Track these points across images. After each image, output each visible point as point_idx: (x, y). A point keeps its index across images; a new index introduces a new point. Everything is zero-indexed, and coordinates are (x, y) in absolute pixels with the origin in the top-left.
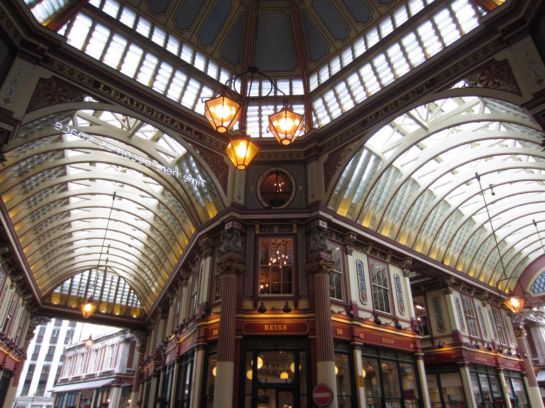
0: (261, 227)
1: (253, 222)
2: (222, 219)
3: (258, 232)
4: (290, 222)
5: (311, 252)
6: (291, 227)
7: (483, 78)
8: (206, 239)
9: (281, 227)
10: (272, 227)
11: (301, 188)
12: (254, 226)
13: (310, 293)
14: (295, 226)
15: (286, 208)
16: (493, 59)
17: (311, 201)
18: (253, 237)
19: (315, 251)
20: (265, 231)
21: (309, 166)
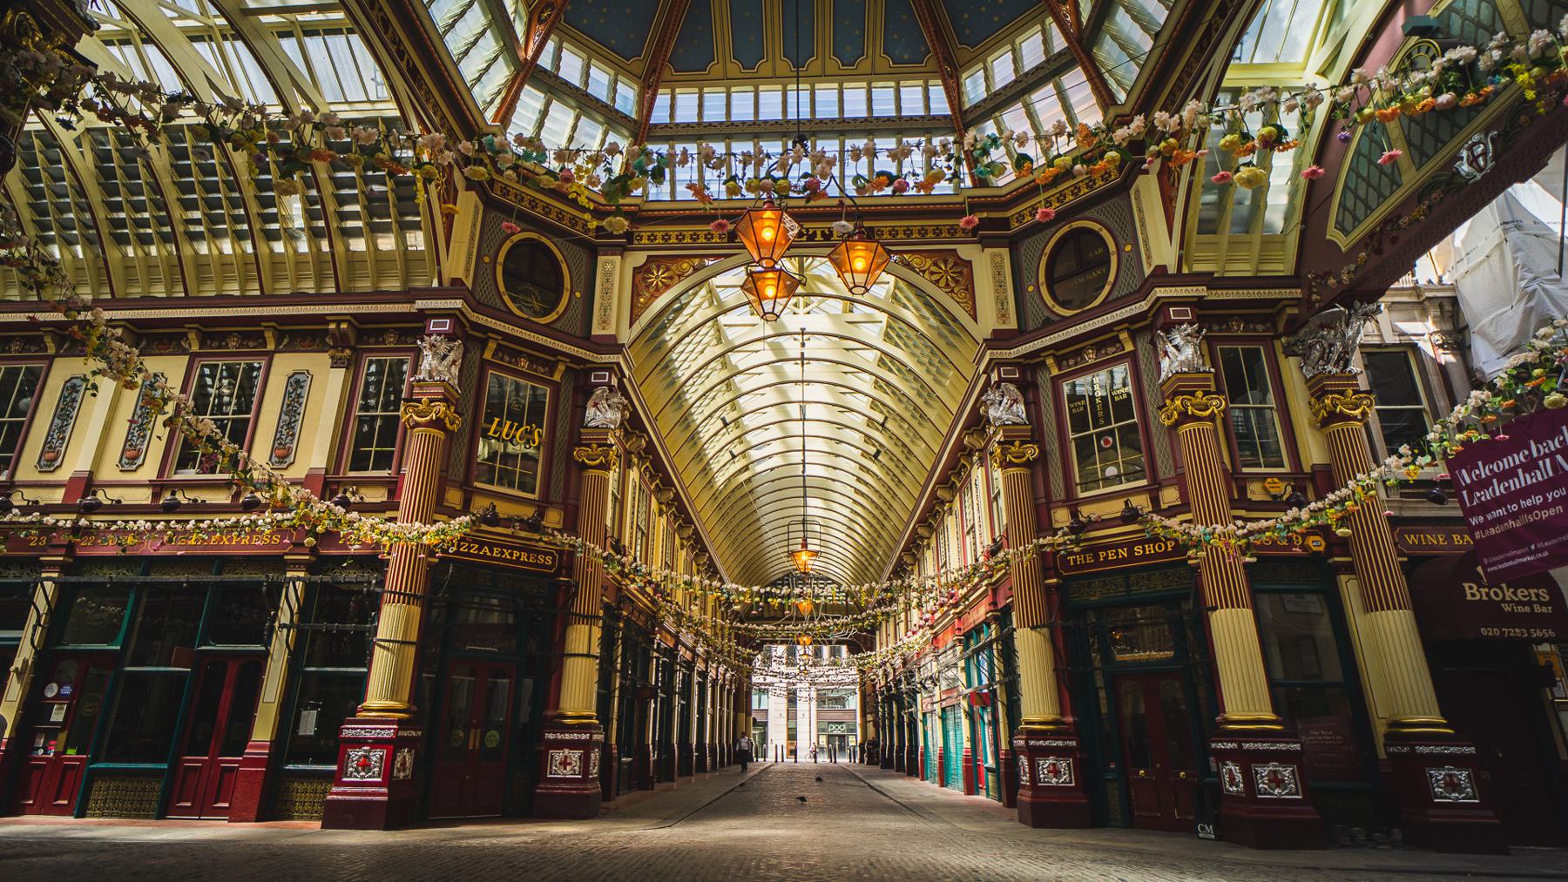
0: (499, 348)
1: (485, 334)
2: (420, 304)
3: (488, 355)
4: (555, 356)
5: (586, 427)
6: (552, 369)
7: (934, 269)
8: (344, 326)
9: (533, 360)
10: (518, 354)
11: (578, 295)
12: (483, 344)
13: (571, 501)
14: (561, 367)
15: (547, 325)
16: (955, 250)
17: (596, 331)
18: (477, 364)
19: (597, 427)
20: (502, 359)
21: (601, 259)
